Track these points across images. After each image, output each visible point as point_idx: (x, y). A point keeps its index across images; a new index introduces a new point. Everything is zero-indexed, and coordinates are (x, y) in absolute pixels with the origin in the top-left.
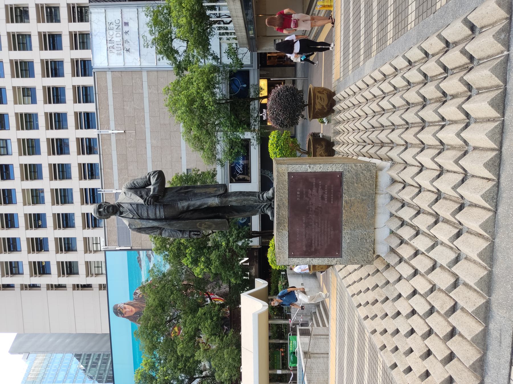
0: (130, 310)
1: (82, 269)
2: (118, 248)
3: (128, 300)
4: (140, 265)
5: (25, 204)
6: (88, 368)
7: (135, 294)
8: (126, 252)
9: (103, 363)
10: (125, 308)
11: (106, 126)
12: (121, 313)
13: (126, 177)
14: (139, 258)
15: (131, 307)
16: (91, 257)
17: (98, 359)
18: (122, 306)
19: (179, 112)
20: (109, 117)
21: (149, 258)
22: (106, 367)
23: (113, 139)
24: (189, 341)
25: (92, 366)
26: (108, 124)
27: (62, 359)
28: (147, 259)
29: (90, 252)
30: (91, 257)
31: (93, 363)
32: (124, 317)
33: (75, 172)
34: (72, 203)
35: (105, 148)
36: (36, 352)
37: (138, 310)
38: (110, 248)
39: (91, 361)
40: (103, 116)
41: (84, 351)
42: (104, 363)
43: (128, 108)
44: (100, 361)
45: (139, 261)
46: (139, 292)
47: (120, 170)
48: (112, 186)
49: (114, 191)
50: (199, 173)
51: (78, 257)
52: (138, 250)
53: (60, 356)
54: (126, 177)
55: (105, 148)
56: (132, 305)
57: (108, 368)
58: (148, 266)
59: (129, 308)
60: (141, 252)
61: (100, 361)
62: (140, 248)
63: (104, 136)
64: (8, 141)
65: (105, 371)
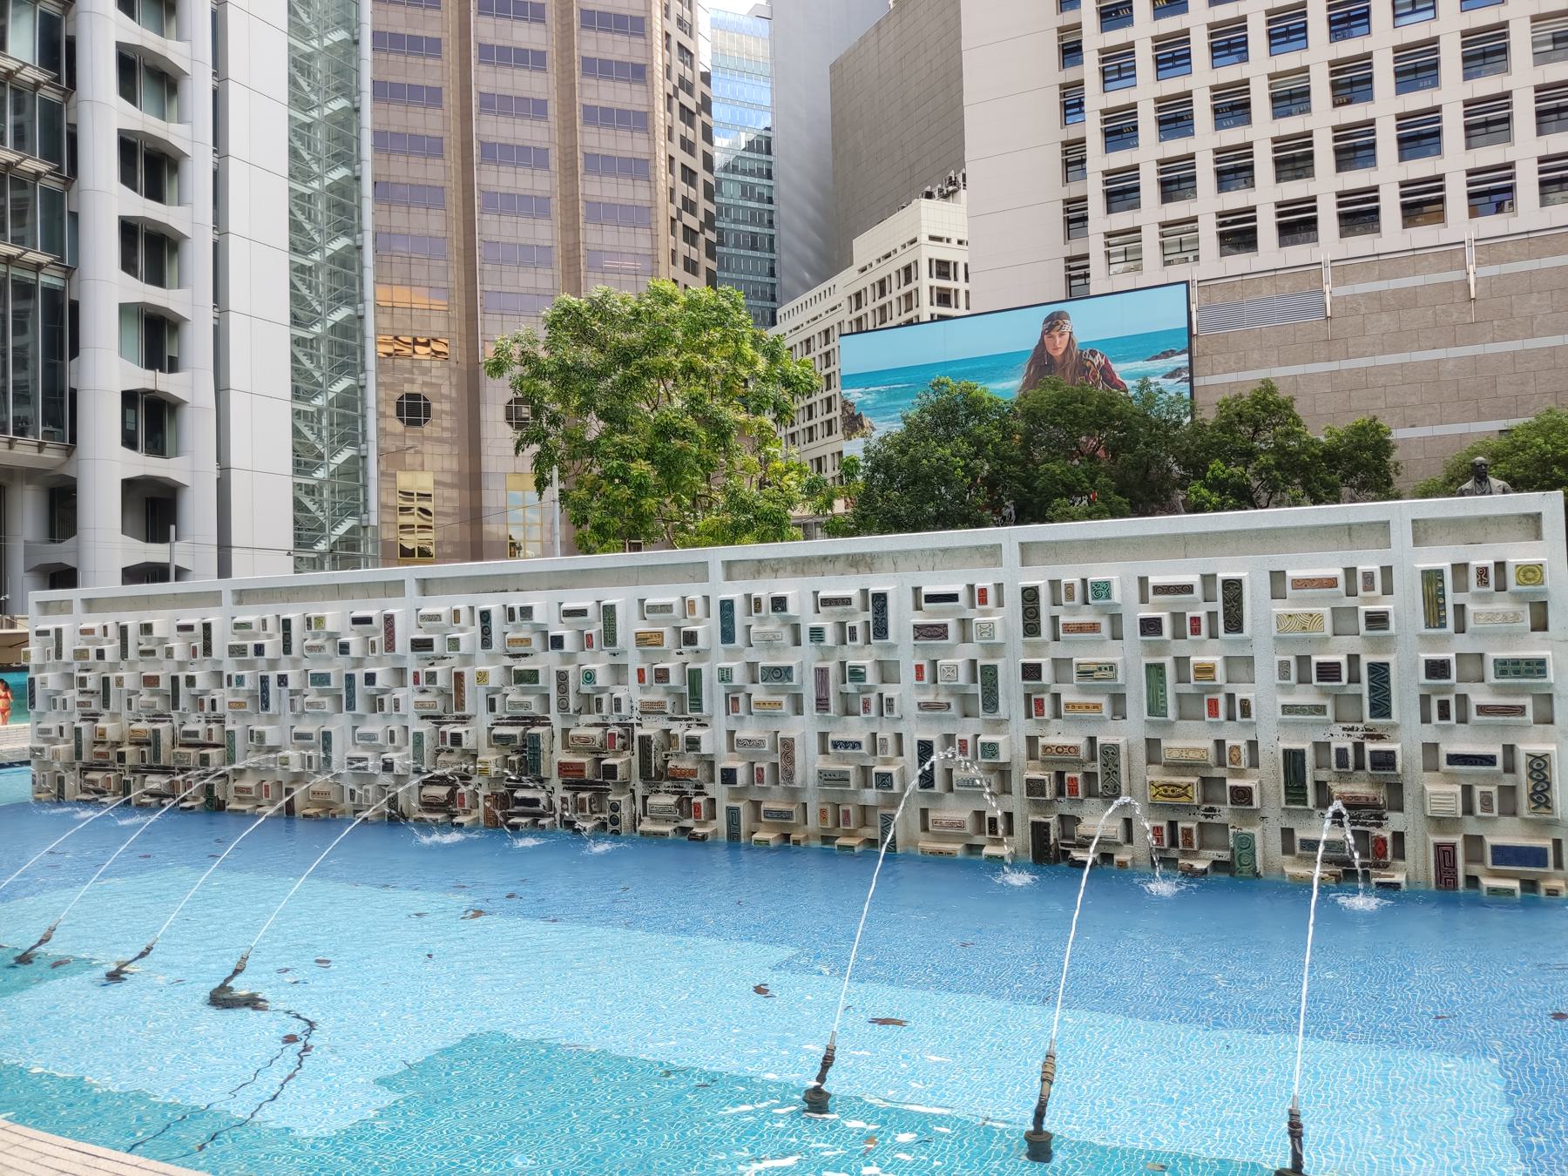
0: (1059, 345)
1: (1122, 220)
2: (1194, 308)
3: (1079, 339)
4: (1157, 358)
5: (1271, 77)
6: (740, 178)
7: (1093, 353)
8: (1185, 325)
9: (753, 211)
10: (1061, 335)
11: (1485, 257)
12: (1051, 328)
13: (1363, 310)
14: (1173, 353)
15: (1064, 346)
16: (1150, 239)
17: (760, 199)
18: (1067, 329)
19: (1540, 440)
20: (1509, 261)
21: (1171, 375)
22: (744, 222)
23: (1456, 276)
24: (1064, 485)
25: (744, 186)
26: (1491, 262)
27: (758, 107)
28: (1169, 370)
29: (1162, 235)
30: (1150, 239)
31: (753, 186)
32: (1043, 333)
33: (1356, 179)
34: (1278, 180)
35: (1431, 259)
36: (773, 36)
37: (1059, 360)
38: (1194, 292)
39: (756, 180)
40: (1509, 248)
41: (780, 160)
42: (753, 216)
43: (1534, 302)
44: (756, 205)
45: (1166, 355)
46: (1098, 360)
47: (1378, 296)
48: (1337, 282)
49: (1327, 288)
50: (1393, 475)
51: (1151, 211)
52: (1190, 351)
53: (765, 98)
54: (1363, 310)
55: (1431, 259)
56: (1068, 348)
57: (742, 227)
58: (1154, 374)
59: (1061, 343)
60: (1186, 356)
61: (756, 205)
62: (1195, 354)
63: (1460, 255)
64: (1430, 14)
65: (735, 221)
